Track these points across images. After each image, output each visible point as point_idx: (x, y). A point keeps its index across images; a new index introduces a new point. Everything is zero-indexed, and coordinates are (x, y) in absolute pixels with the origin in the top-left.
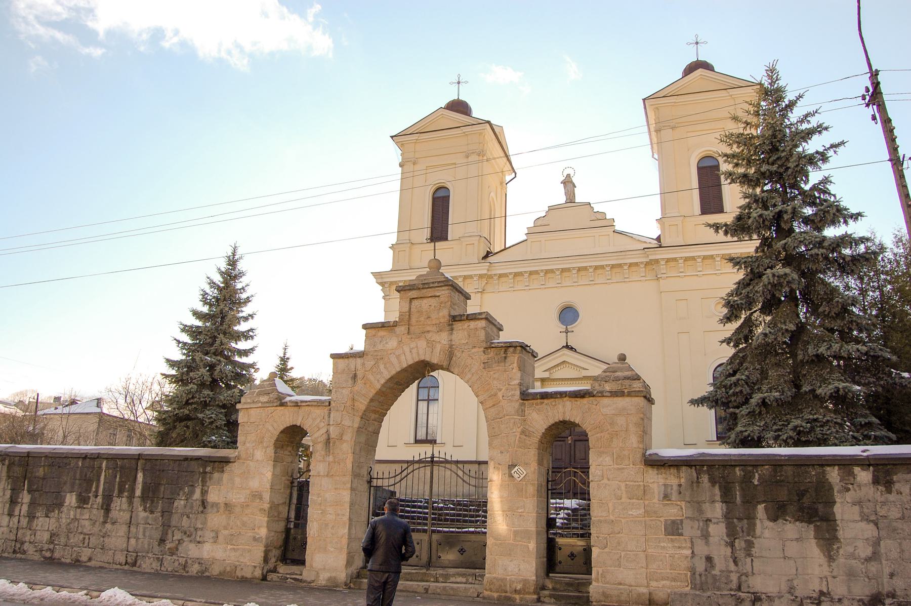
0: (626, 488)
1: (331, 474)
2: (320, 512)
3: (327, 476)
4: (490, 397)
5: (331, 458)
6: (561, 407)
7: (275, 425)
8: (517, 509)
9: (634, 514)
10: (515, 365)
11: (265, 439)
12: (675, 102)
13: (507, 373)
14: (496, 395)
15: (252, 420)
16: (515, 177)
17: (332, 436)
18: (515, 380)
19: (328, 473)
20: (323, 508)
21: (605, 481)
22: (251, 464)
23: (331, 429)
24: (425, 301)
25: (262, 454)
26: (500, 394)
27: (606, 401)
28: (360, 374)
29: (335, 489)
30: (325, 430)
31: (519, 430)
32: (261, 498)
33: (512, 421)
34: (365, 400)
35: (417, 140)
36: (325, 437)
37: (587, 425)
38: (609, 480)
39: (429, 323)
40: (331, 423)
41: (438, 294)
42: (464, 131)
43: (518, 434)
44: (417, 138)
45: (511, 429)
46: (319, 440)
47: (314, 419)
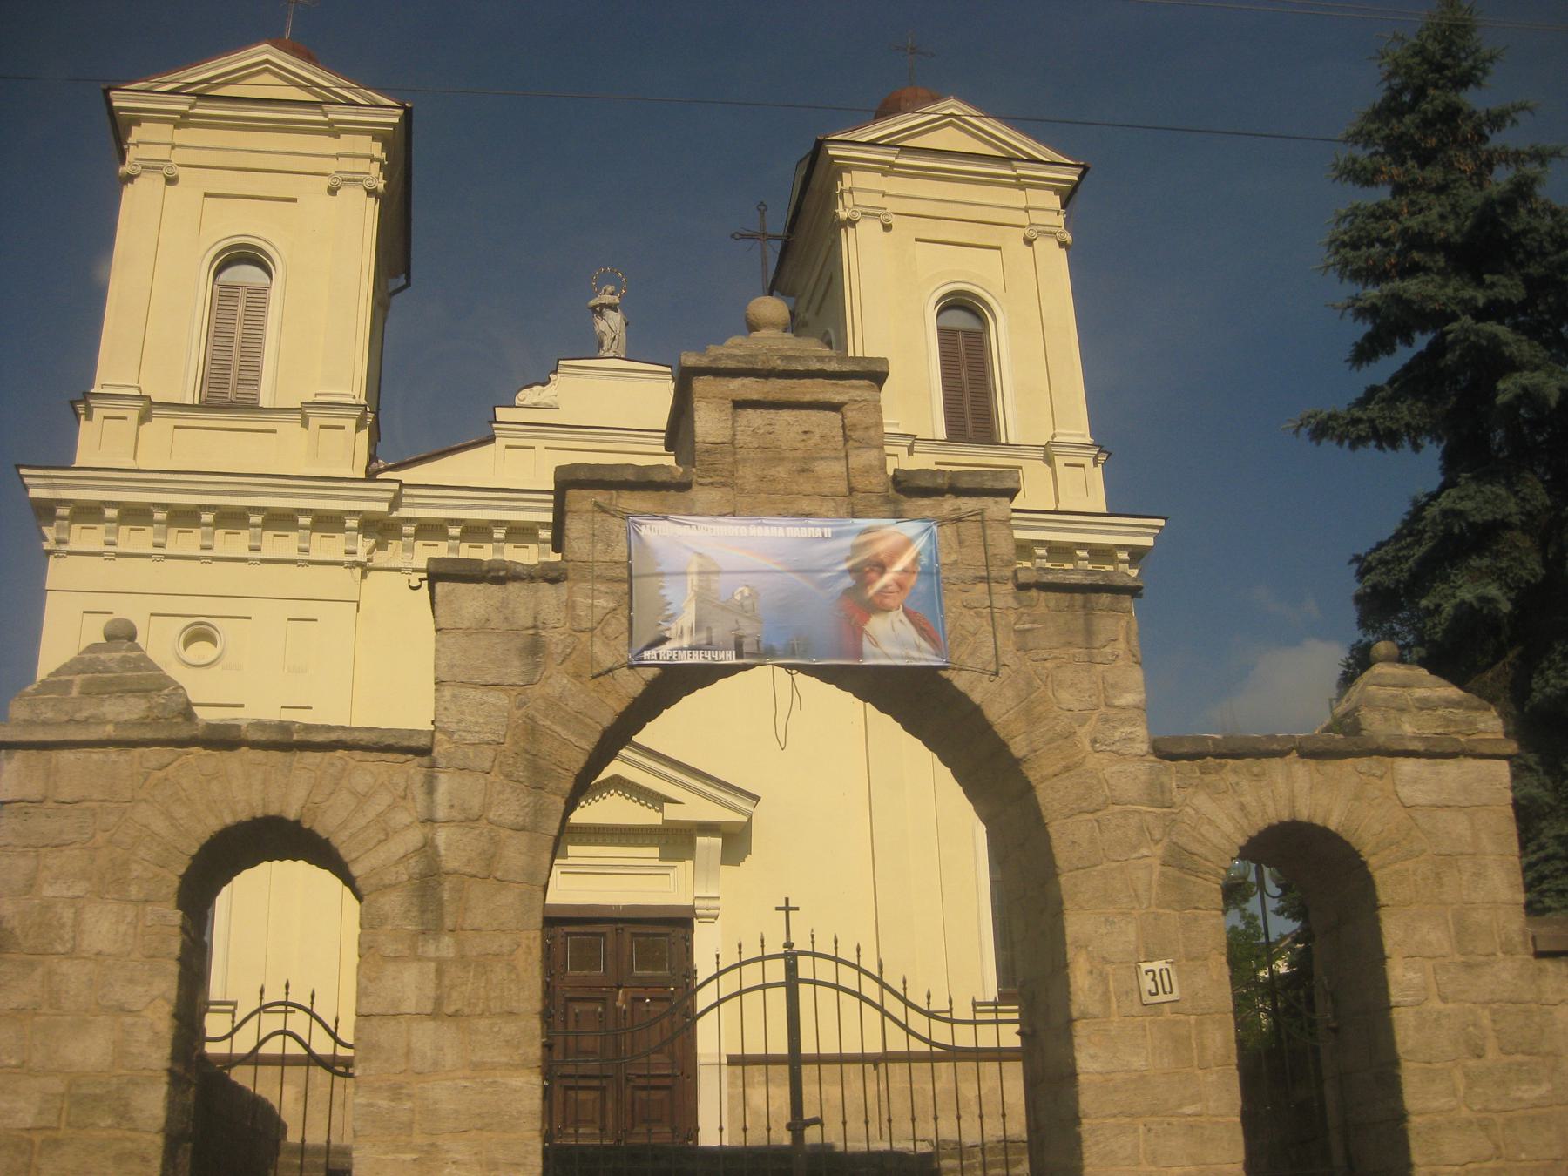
0: (1494, 1021)
1: (451, 1009)
2: (409, 1157)
3: (434, 1015)
4: (1052, 740)
5: (446, 947)
6: (1280, 780)
7: (180, 812)
8: (1180, 1106)
9: (1526, 1096)
10: (1121, 646)
11: (136, 870)
12: (892, 165)
13: (1100, 667)
14: (1069, 735)
15: (66, 793)
16: (408, 284)
17: (450, 862)
18: (1127, 690)
19: (438, 1002)
20: (419, 1139)
21: (1436, 1004)
22: (66, 967)
23: (442, 837)
24: (786, 415)
25: (122, 928)
26: (1084, 734)
27: (1407, 766)
28: (555, 638)
29: (477, 1067)
30: (414, 838)
31: (1159, 850)
32: (123, 1113)
33: (1134, 820)
34: (583, 736)
35: (184, 115)
36: (415, 866)
37: (1365, 839)
38: (1444, 1000)
39: (808, 488)
40: (441, 813)
41: (837, 398)
42: (332, 116)
43: (1158, 869)
44: (185, 108)
45: (1135, 848)
46: (389, 878)
47: (363, 798)
